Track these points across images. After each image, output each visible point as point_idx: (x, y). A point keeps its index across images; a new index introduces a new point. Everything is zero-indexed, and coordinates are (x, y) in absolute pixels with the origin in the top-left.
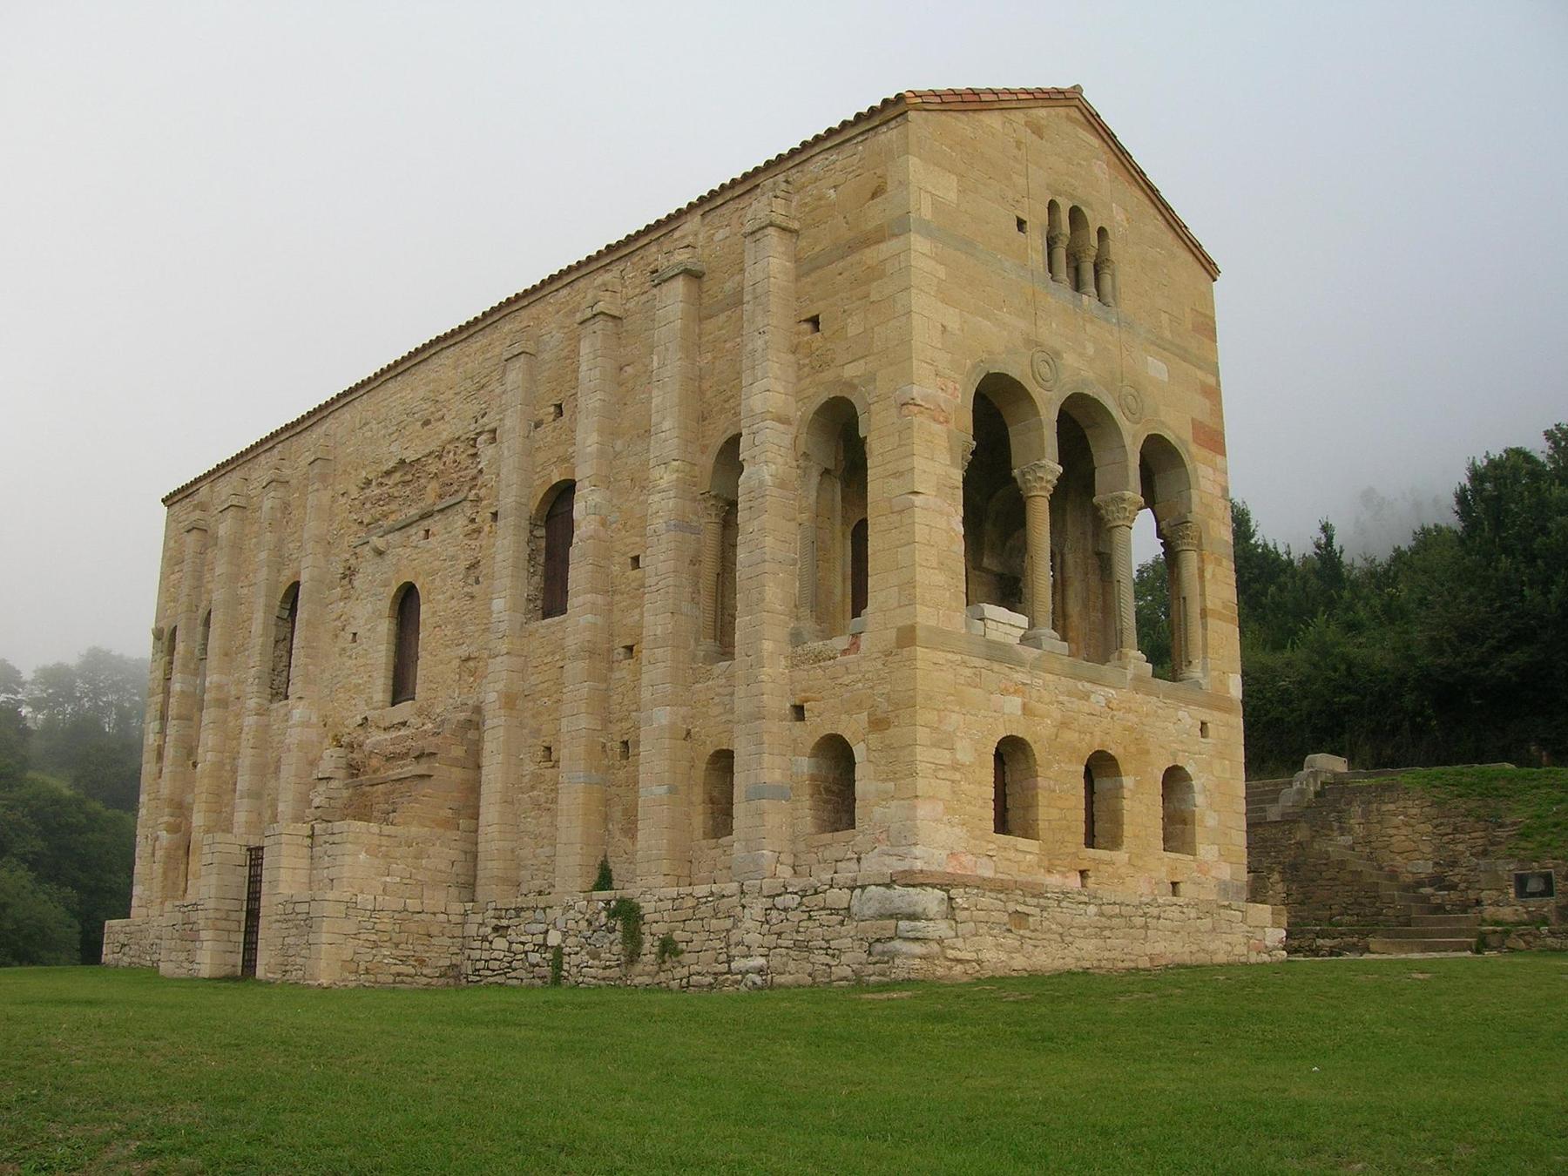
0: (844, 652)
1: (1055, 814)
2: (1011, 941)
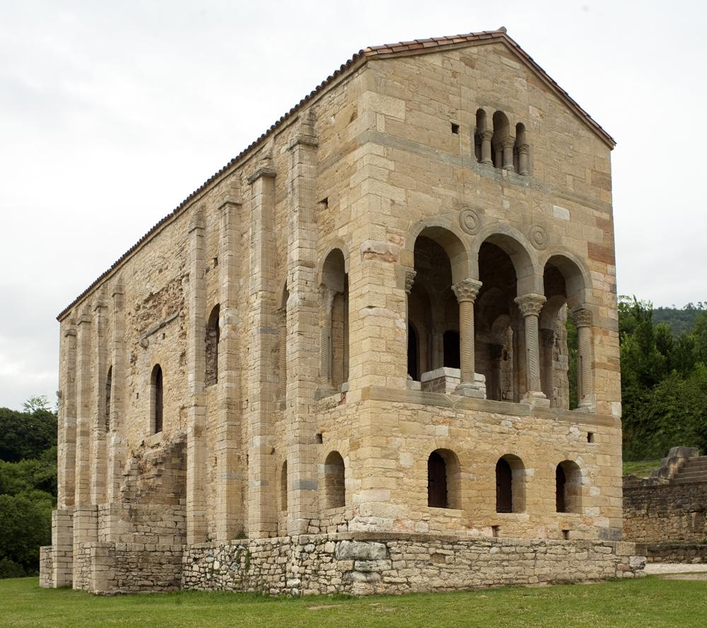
0: (340, 403)
1: (473, 493)
2: (432, 571)
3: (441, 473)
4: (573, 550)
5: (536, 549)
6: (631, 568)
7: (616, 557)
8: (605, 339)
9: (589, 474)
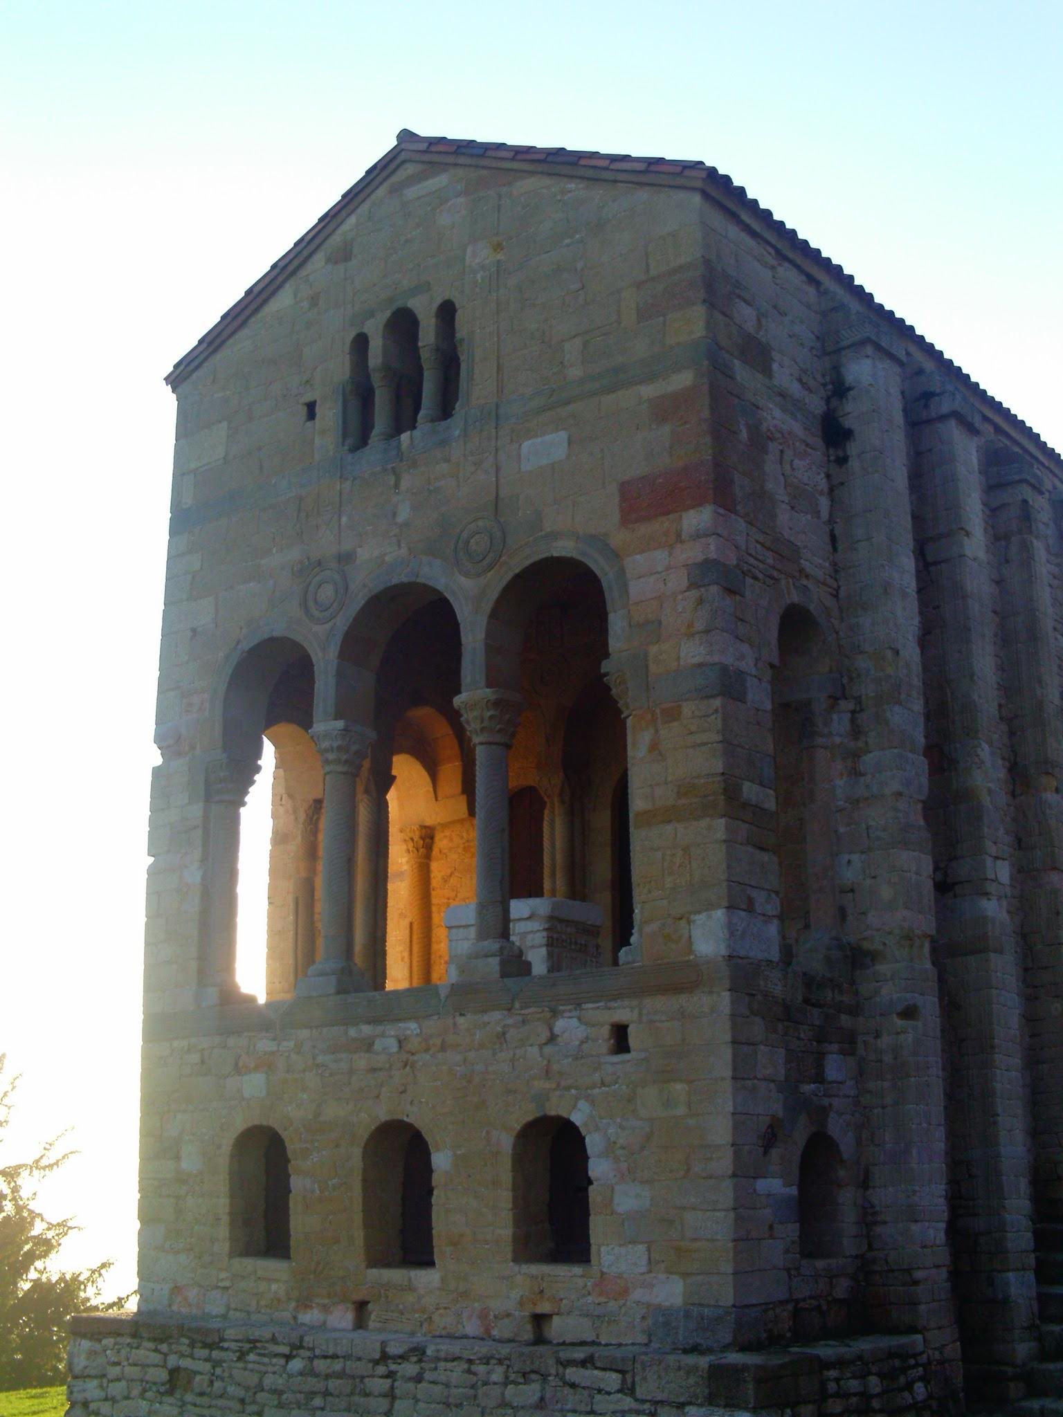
5: (393, 1367)
7: (634, 1405)
9: (610, 1149)
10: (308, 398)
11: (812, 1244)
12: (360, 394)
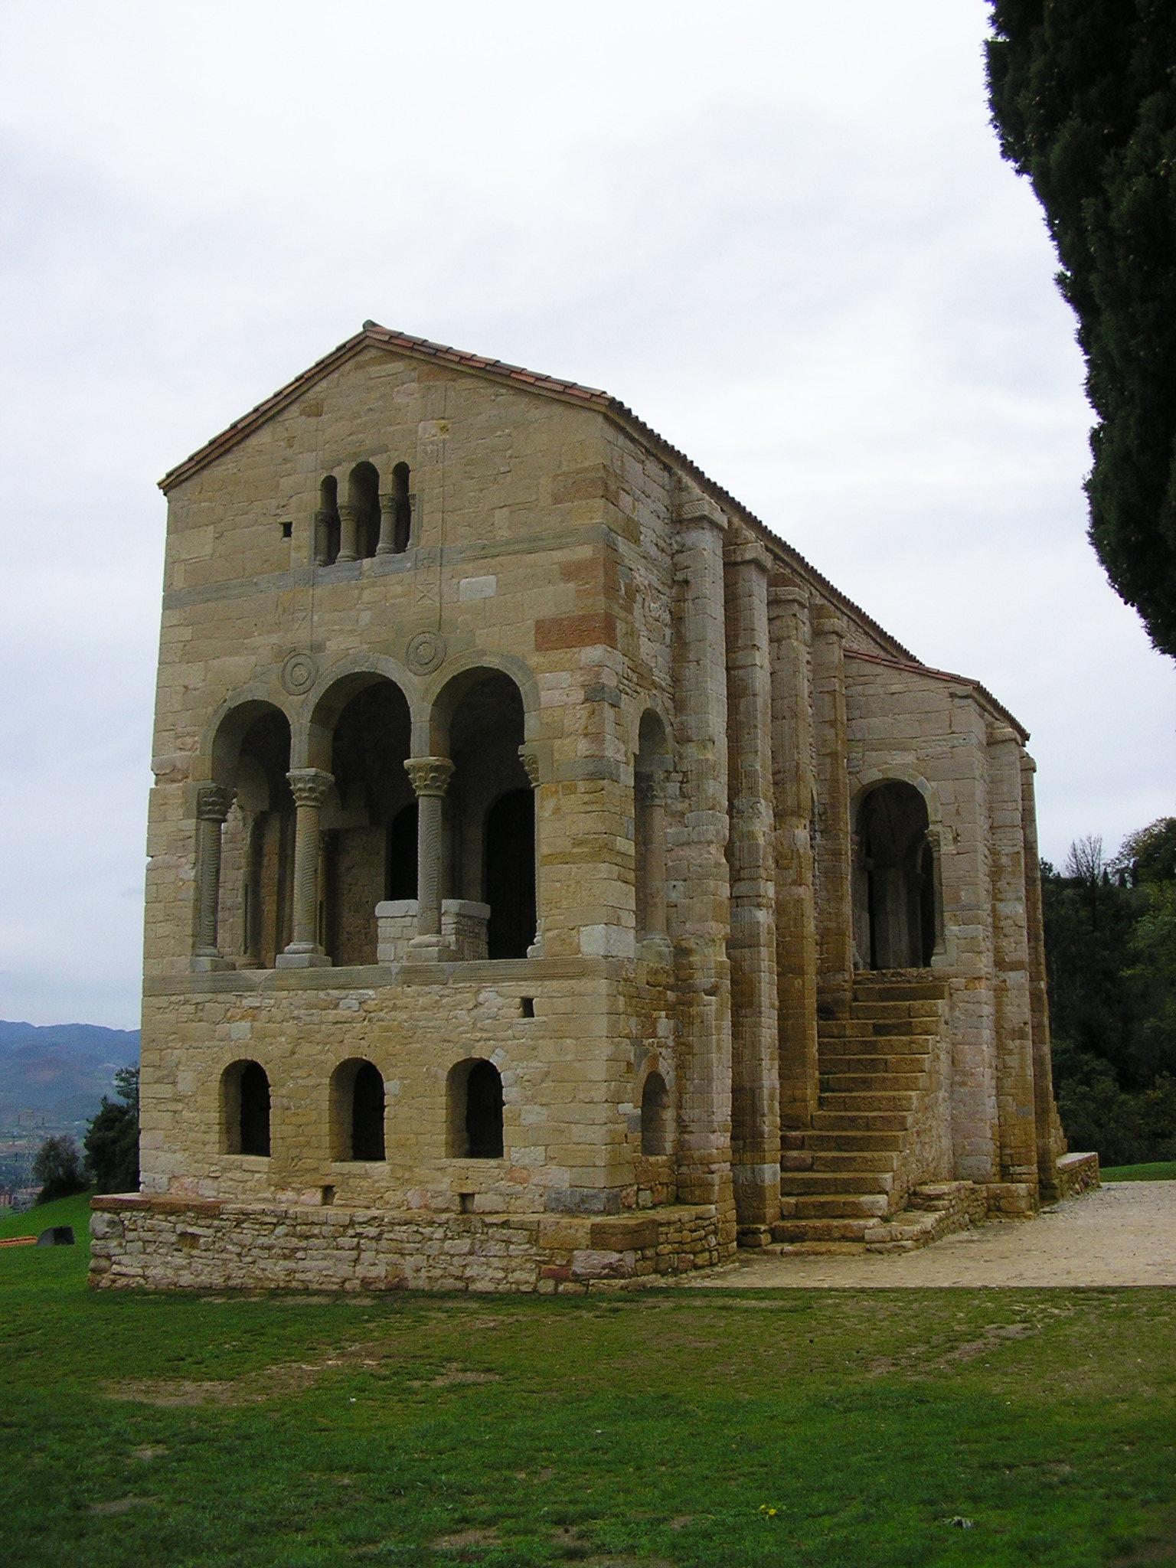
1: (289, 1130)
2: (179, 1260)
3: (248, 1094)
4: (439, 1234)
6: (574, 1274)
8: (570, 802)
10: (285, 519)
11: (650, 1146)
12: (329, 521)
